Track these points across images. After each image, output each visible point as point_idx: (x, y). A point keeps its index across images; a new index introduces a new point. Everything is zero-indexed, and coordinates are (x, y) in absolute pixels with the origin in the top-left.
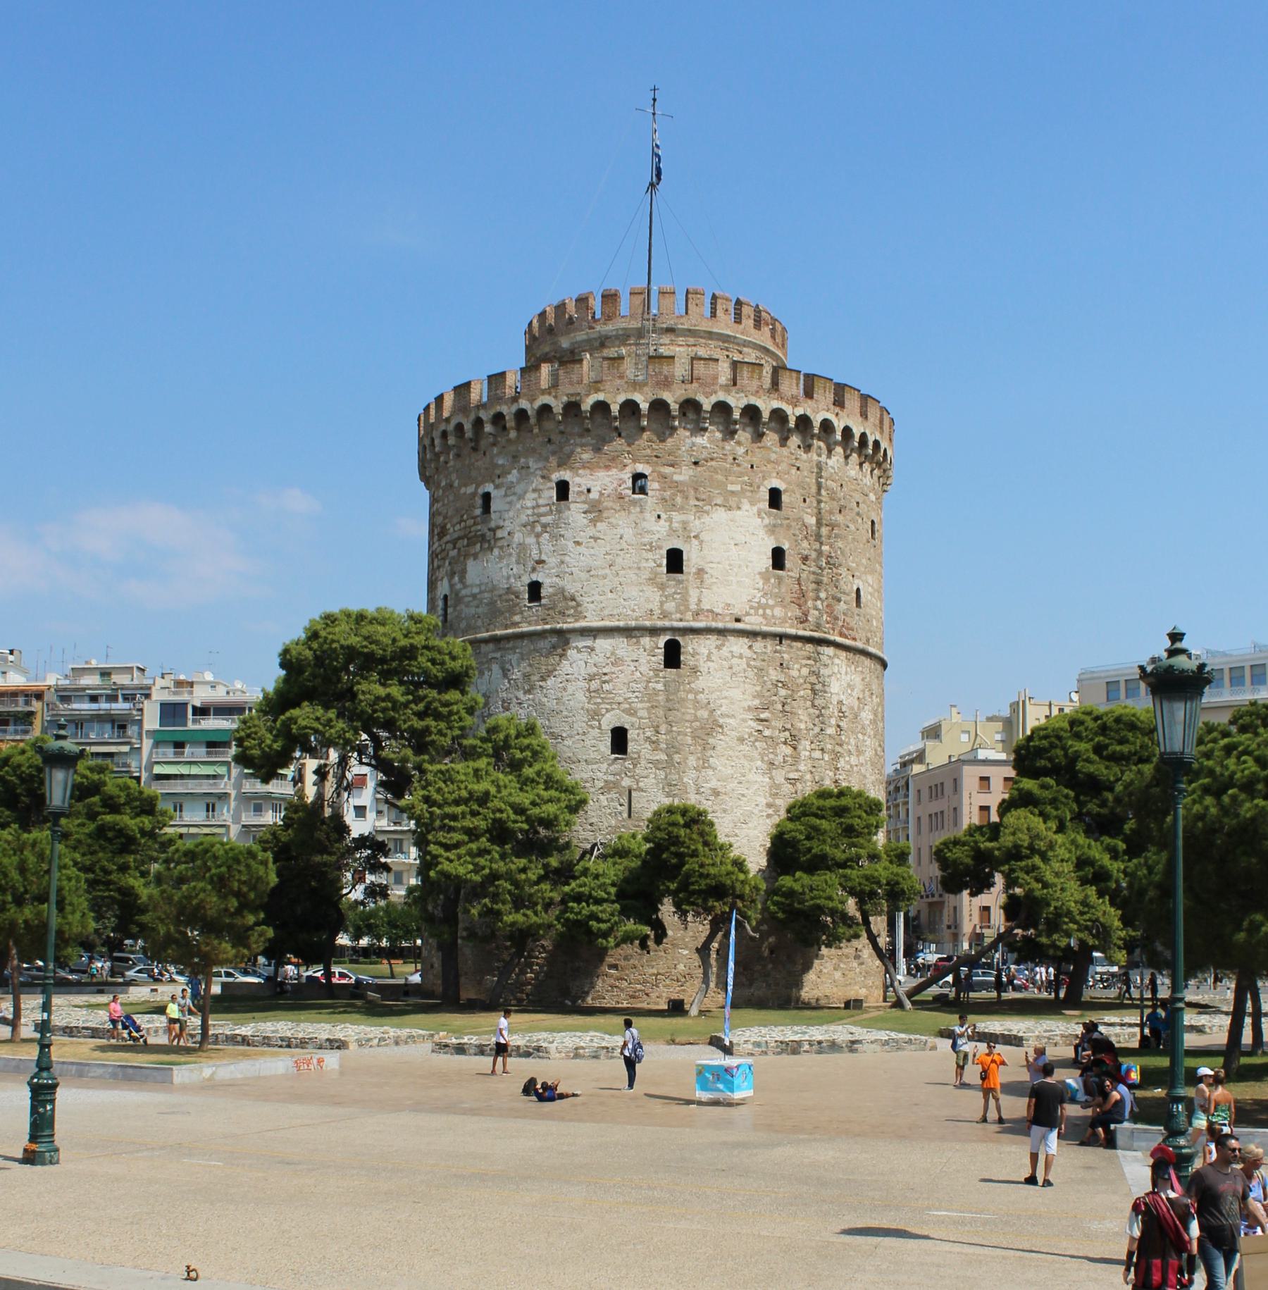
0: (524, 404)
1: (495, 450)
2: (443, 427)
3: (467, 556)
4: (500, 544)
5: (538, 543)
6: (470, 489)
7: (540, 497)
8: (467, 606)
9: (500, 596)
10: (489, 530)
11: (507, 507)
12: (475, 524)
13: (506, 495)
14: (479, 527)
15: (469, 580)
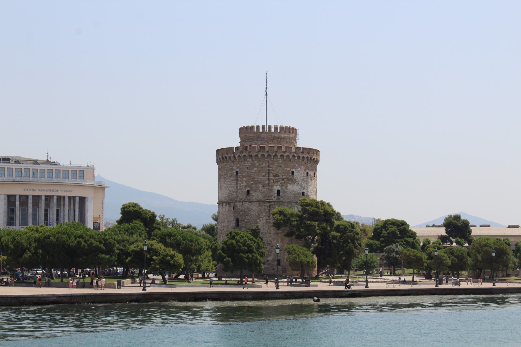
0: (304, 155)
1: (295, 163)
2: (282, 154)
3: (288, 183)
4: (297, 182)
5: (304, 184)
6: (288, 169)
7: (304, 175)
8: (288, 194)
9: (297, 193)
10: (294, 179)
11: (298, 175)
12: (290, 177)
13: (298, 173)
14: (291, 178)
15: (288, 189)
